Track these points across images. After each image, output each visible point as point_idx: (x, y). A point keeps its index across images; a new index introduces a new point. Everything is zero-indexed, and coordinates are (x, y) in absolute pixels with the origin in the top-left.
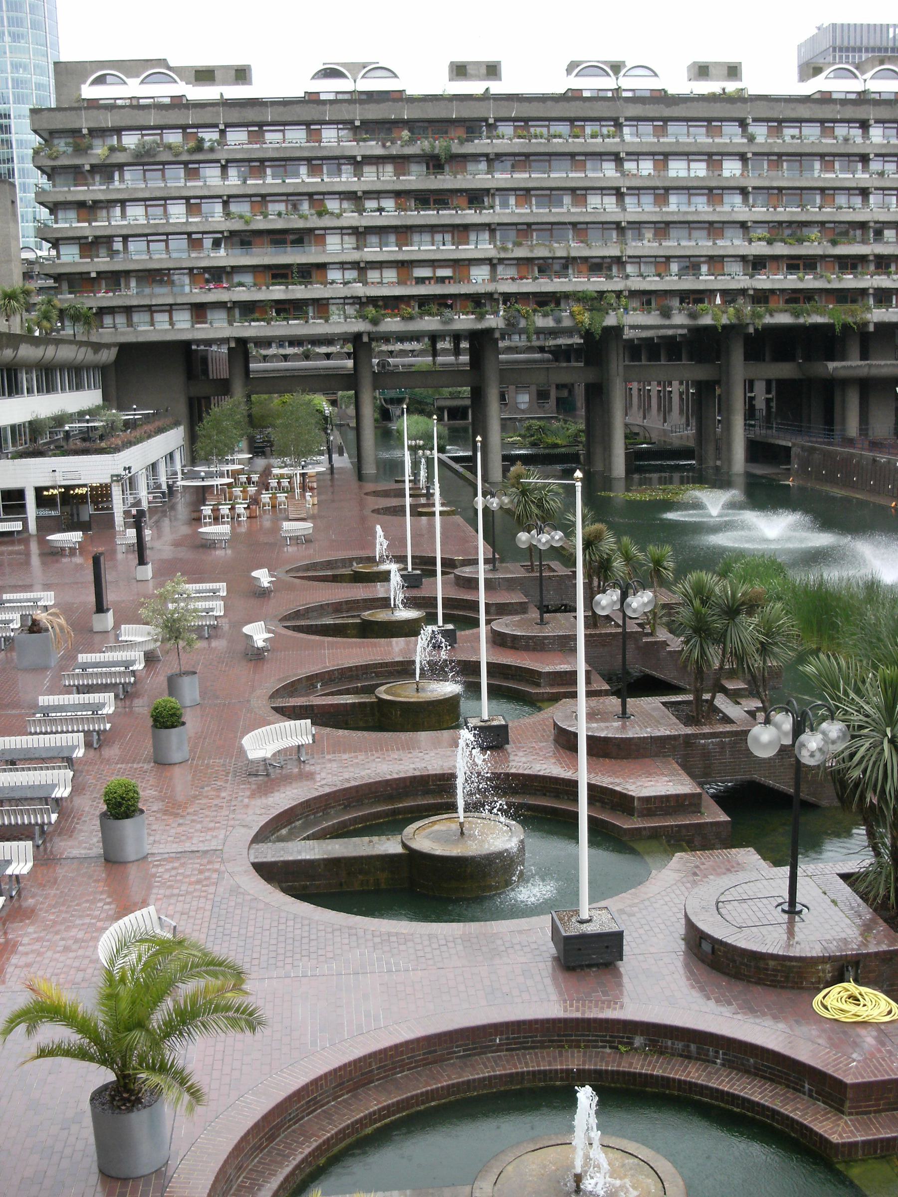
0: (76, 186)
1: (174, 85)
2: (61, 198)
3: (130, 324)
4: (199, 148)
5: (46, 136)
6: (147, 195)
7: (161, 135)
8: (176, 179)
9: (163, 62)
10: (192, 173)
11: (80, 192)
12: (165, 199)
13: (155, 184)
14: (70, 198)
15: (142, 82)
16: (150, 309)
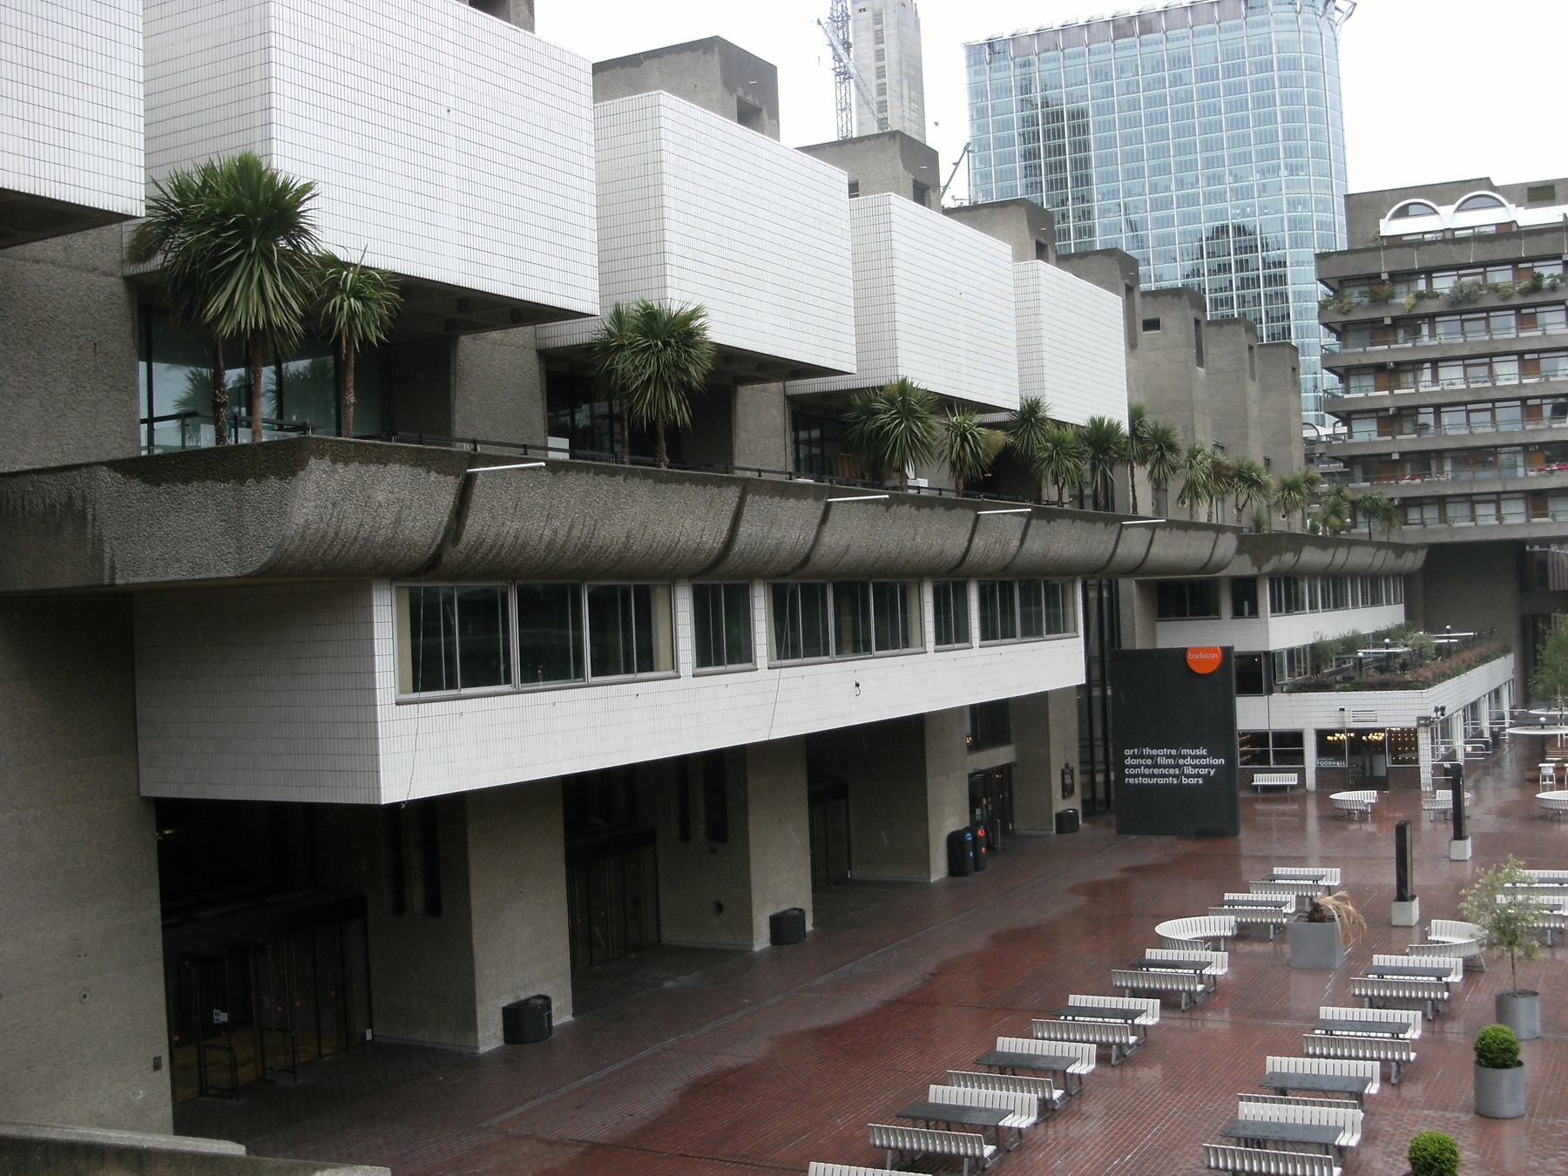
0: (1373, 345)
1: (1501, 210)
2: (1354, 362)
3: (1443, 518)
4: (1536, 287)
5: (1336, 286)
6: (1466, 352)
7: (1484, 274)
8: (1505, 329)
9: (1485, 182)
10: (1526, 320)
11: (1380, 352)
12: (1491, 356)
13: (1477, 336)
14: (1365, 361)
15: (1458, 210)
16: (1471, 500)
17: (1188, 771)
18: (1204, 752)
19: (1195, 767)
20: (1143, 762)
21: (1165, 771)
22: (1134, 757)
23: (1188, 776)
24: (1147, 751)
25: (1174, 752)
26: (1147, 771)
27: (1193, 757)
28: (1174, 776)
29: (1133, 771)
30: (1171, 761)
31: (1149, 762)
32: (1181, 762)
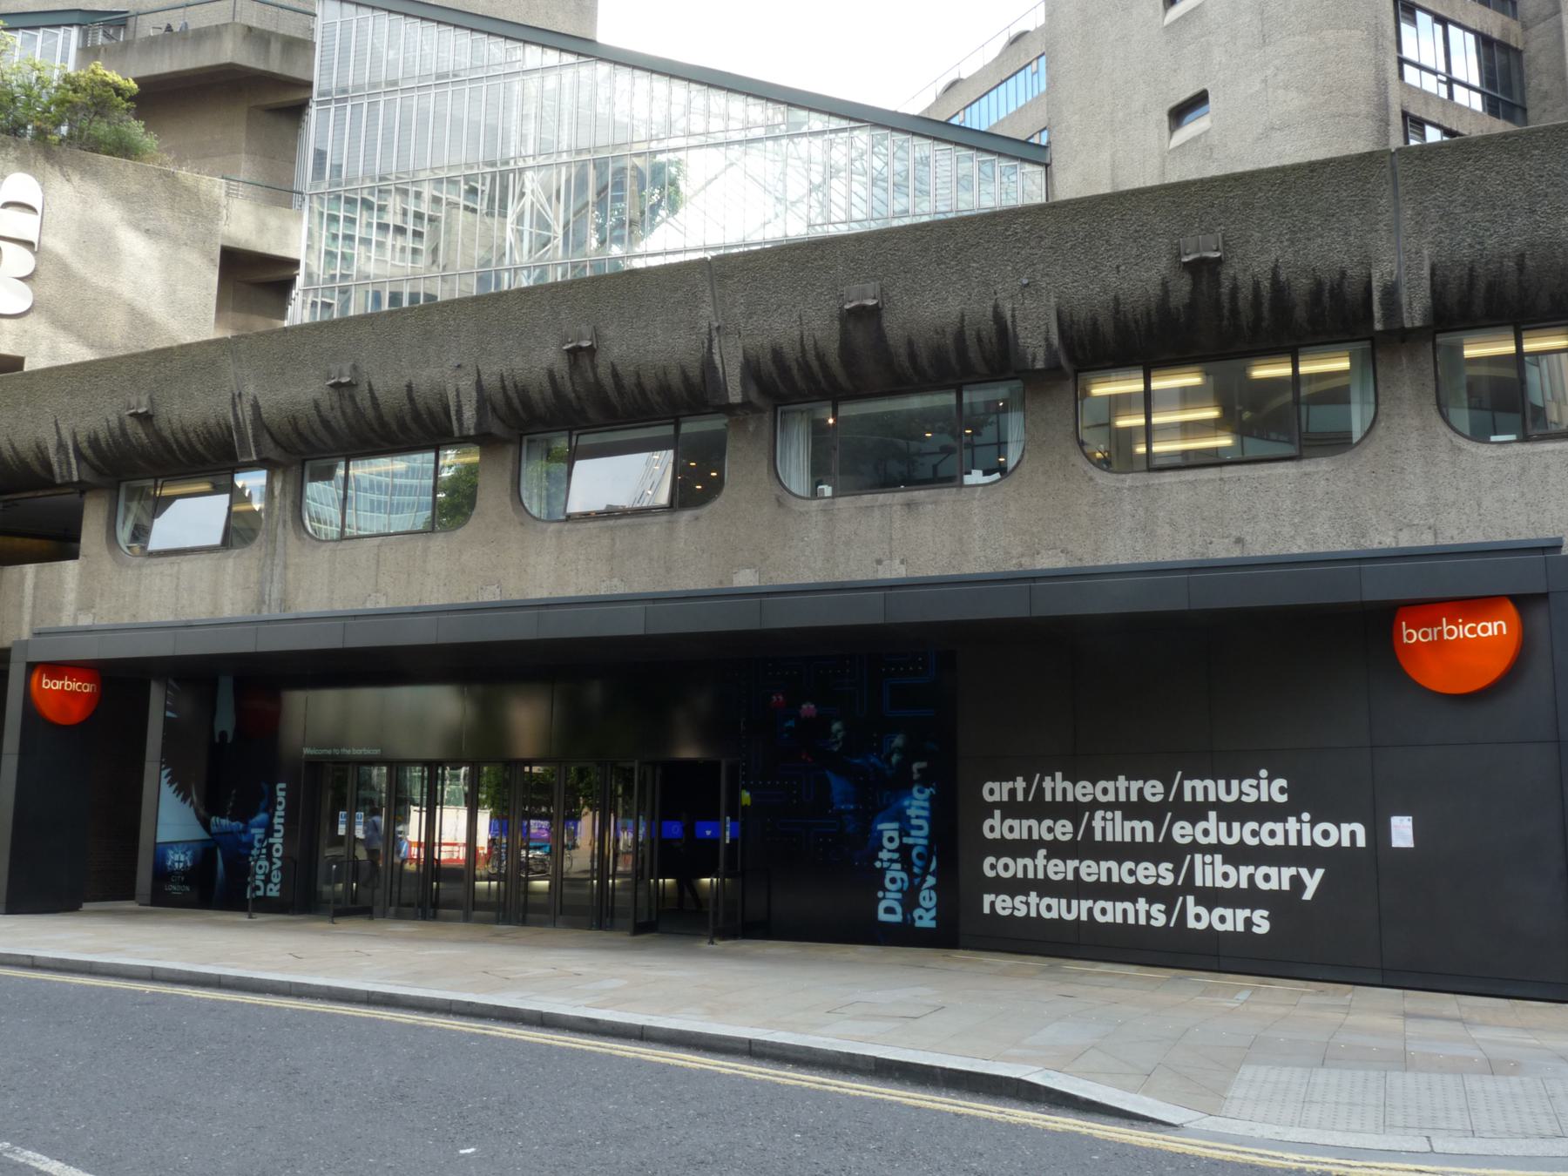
17: (1212, 872)
18: (1274, 790)
19: (1237, 855)
20: (1040, 829)
21: (1121, 872)
22: (1012, 809)
23: (1211, 897)
24: (1056, 787)
25: (1154, 791)
26: (1059, 870)
27: (1233, 812)
28: (1154, 893)
29: (1014, 867)
30: (1143, 830)
31: (1063, 830)
32: (1182, 832)
